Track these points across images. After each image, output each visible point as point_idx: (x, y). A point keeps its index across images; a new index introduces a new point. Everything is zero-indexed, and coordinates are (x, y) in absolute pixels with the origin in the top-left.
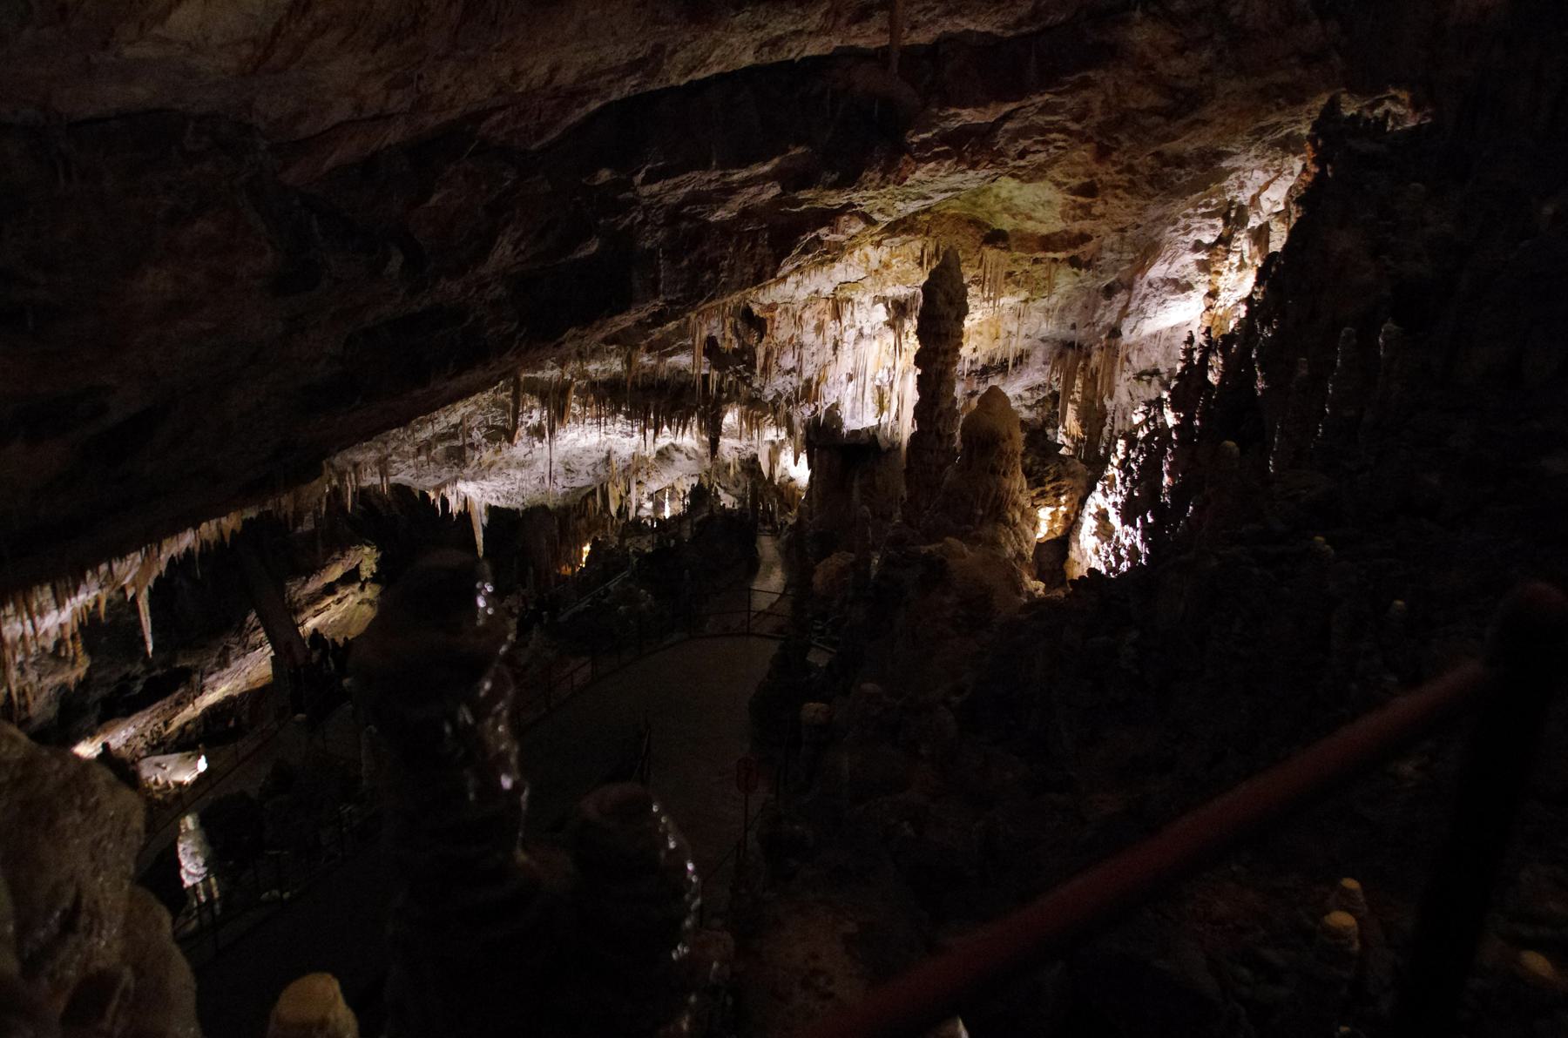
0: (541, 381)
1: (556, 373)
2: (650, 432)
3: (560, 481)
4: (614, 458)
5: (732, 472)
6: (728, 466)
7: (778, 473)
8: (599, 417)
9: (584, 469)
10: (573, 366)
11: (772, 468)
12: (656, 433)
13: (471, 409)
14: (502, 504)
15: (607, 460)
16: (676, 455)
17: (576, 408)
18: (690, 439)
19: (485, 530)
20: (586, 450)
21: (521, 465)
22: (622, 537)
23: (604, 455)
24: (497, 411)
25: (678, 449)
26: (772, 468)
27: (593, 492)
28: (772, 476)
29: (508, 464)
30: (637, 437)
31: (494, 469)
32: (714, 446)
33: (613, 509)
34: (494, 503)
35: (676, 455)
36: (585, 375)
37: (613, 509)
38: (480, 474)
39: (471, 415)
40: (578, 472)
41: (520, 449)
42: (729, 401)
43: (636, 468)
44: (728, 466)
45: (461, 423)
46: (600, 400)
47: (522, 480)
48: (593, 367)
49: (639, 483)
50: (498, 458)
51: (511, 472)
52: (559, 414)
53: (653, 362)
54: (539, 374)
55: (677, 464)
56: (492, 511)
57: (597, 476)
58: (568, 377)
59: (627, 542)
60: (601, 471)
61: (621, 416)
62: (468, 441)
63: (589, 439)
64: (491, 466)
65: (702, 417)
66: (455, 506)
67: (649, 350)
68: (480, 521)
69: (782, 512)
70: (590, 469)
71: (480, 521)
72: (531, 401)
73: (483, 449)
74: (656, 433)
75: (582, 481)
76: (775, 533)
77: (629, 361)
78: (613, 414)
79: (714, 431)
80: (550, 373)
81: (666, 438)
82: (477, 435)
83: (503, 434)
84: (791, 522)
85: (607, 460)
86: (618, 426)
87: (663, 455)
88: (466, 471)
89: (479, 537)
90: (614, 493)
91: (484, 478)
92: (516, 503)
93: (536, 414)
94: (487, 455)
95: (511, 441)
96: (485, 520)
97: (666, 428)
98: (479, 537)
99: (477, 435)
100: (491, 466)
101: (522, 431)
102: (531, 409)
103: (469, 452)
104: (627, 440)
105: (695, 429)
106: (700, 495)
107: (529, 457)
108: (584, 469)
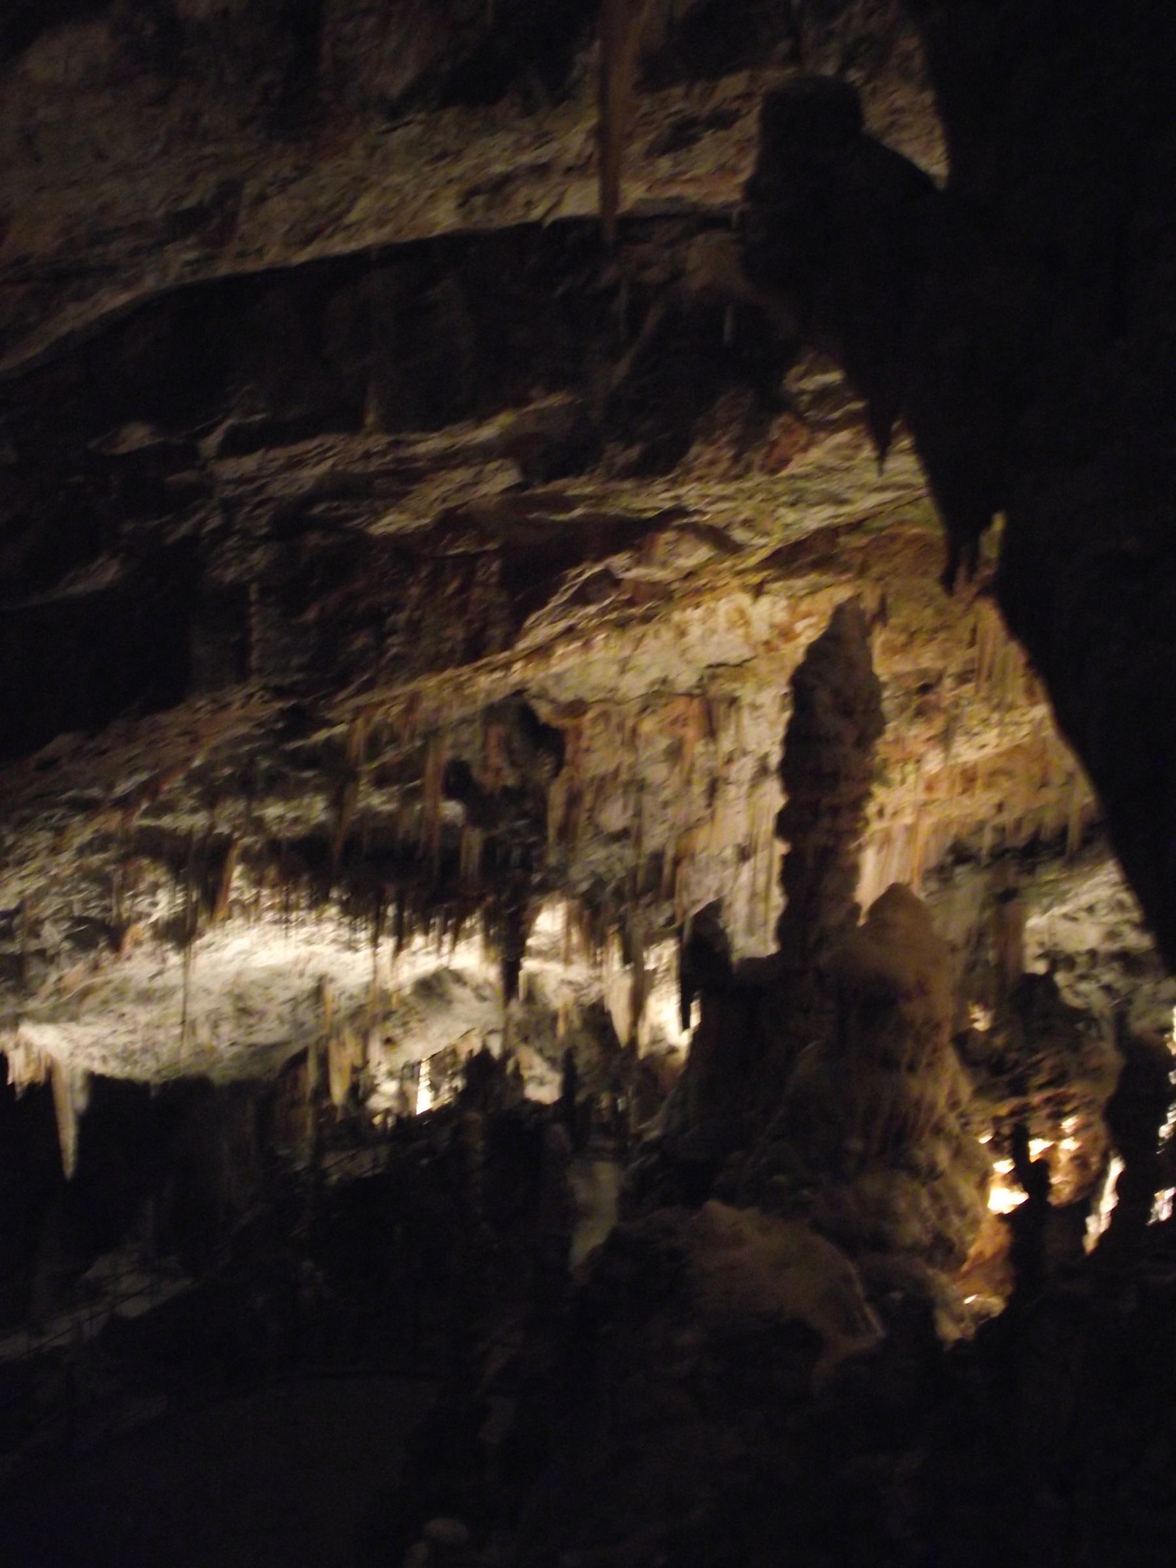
0: (172, 834)
1: (199, 821)
2: (387, 944)
3: (225, 1029)
4: (330, 991)
5: (561, 1028)
6: (554, 1018)
7: (644, 1038)
8: (287, 908)
9: (274, 1010)
10: (232, 808)
11: (635, 1023)
12: (399, 948)
13: (42, 882)
14: (113, 1069)
15: (318, 993)
16: (457, 991)
17: (343, 883)
18: (471, 957)
19: (85, 1121)
20: (278, 974)
21: (146, 997)
22: (320, 1148)
23: (308, 984)
24: (91, 890)
25: (458, 978)
26: (635, 1023)
27: (300, 1059)
28: (633, 1042)
29: (120, 993)
30: (366, 951)
31: (92, 1001)
32: (511, 970)
33: (339, 1091)
34: (99, 1068)
35: (457, 991)
36: (258, 825)
37: (339, 1091)
38: (66, 1009)
39: (40, 894)
40: (262, 1015)
41: (139, 964)
42: (545, 889)
43: (376, 1014)
44: (554, 1018)
45: (18, 911)
46: (288, 878)
47: (147, 1025)
48: (273, 811)
49: (389, 1042)
50: (98, 980)
51: (127, 1008)
52: (208, 900)
53: (390, 807)
54: (167, 821)
55: (458, 1008)
56: (97, 1084)
57: (299, 1025)
58: (223, 829)
59: (329, 1160)
60: (306, 1015)
61: (333, 911)
62: (33, 945)
63: (278, 953)
64: (86, 993)
65: (490, 918)
66: (20, 1071)
67: (381, 781)
68: (71, 1102)
69: (647, 1112)
70: (286, 1008)
71: (71, 1102)
72: (155, 874)
73: (63, 959)
74: (399, 948)
75: (270, 1032)
76: (620, 1156)
77: (337, 803)
78: (318, 901)
79: (510, 945)
80: (189, 821)
81: (423, 957)
82: (52, 934)
83: (102, 934)
84: (654, 1134)
85: (318, 993)
86: (328, 929)
87: (432, 989)
88: (32, 1005)
89: (69, 1135)
90: (344, 1057)
91: (74, 1018)
92: (144, 1070)
93: (163, 897)
94: (74, 973)
95: (116, 945)
96: (81, 1101)
97: (418, 941)
98: (69, 1135)
99: (52, 934)
100: (86, 993)
101: (141, 929)
102: (155, 888)
103: (35, 969)
104: (348, 956)
105: (478, 939)
106: (484, 1074)
107: (159, 982)
108: (274, 1010)
